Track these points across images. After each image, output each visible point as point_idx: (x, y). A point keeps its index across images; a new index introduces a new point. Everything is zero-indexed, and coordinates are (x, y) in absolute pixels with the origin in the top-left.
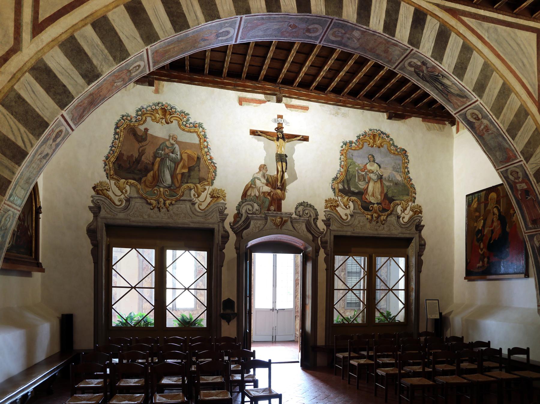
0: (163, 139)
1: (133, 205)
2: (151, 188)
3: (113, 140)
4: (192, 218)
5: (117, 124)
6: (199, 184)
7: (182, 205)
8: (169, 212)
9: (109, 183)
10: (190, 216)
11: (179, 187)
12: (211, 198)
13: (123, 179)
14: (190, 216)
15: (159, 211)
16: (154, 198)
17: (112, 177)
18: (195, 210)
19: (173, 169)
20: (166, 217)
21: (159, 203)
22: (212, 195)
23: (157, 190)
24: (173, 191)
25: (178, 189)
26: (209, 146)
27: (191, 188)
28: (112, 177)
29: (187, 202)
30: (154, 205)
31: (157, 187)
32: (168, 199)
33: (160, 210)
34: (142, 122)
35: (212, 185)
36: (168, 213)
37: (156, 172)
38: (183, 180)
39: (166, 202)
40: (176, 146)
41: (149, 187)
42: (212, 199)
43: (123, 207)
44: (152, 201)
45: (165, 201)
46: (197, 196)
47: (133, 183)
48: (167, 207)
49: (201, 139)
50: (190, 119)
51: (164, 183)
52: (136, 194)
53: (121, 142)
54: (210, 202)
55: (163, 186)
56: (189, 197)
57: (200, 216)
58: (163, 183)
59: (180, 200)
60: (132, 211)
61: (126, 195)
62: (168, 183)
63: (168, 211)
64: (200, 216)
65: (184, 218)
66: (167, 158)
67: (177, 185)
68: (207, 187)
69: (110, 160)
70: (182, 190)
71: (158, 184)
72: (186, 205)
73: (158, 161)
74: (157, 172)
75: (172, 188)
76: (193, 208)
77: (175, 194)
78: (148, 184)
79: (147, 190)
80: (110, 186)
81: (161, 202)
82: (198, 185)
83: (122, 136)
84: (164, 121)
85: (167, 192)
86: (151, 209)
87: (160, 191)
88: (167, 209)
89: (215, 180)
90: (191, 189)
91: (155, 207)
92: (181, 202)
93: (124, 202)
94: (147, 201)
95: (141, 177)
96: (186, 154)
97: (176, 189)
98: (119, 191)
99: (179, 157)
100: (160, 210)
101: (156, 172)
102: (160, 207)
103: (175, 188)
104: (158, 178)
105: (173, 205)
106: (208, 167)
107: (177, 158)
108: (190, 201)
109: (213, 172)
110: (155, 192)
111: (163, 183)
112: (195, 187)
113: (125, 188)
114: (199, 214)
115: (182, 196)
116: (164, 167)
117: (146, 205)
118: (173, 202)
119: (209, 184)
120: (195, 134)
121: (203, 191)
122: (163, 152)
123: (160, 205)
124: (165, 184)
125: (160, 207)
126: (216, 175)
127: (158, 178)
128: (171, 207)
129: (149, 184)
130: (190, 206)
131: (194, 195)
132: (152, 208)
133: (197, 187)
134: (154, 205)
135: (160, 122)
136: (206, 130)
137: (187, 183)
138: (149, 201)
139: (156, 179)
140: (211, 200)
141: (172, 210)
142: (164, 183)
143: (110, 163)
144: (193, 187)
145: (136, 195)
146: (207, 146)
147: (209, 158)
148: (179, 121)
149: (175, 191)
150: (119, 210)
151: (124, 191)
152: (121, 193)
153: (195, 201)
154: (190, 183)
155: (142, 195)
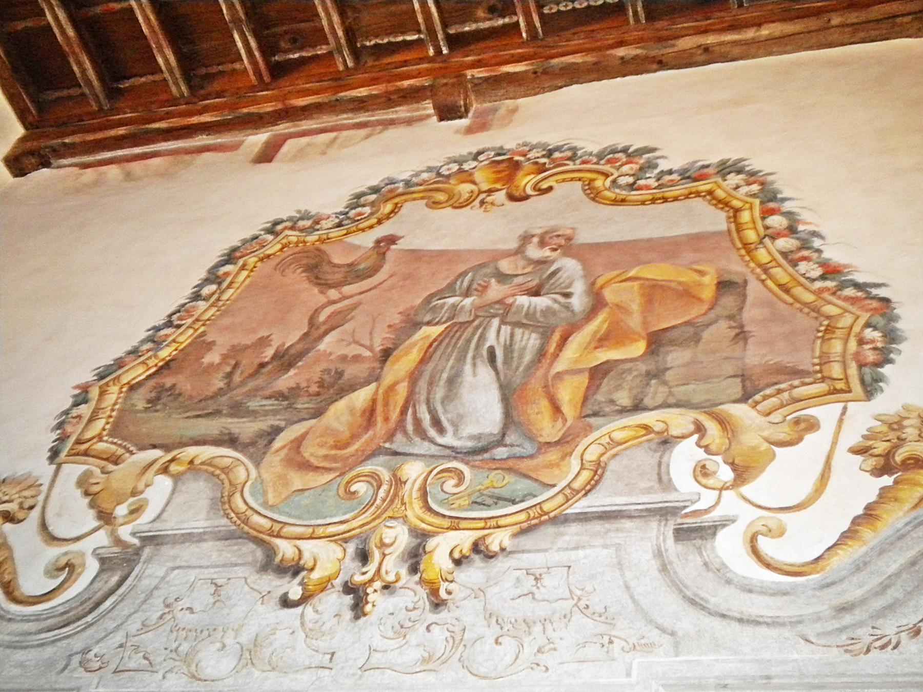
0: (483, 252)
1: (146, 583)
2: (329, 470)
3: (184, 305)
4: (676, 645)
5: (234, 250)
6: (745, 398)
7: (573, 555)
8: (443, 615)
9: (46, 481)
10: (663, 630)
11: (566, 442)
12: (879, 472)
13: (154, 447)
14: (663, 630)
15: (348, 615)
16: (332, 530)
17: (83, 447)
18: (722, 574)
19: (527, 358)
20: (413, 655)
21: (364, 557)
22: (888, 456)
23: (375, 480)
24: (510, 470)
25: (553, 455)
26: (801, 228)
27: (674, 432)
28: (83, 447)
29: (627, 524)
30: (316, 575)
31: (382, 459)
32: (455, 524)
33: (358, 608)
34: (375, 221)
35: (870, 388)
36: (432, 617)
37: (392, 388)
38: (600, 397)
39: (431, 544)
40: (570, 266)
41: (316, 469)
42: (887, 480)
43: (61, 609)
44: (307, 546)
45: (420, 536)
46: (726, 474)
47: (209, 463)
48: (430, 575)
49: (737, 211)
50: (659, 161)
51: (441, 430)
52: (203, 515)
53: (221, 303)
54: (868, 508)
55: (434, 450)
56: (649, 490)
57: (774, 623)
58: (432, 433)
59: (560, 520)
60: (117, 628)
61: (124, 532)
62: (470, 429)
63: (438, 604)
64: (774, 623)
65: (592, 651)
66: (494, 316)
67: (549, 430)
68: (826, 413)
69: (118, 378)
70: (589, 456)
71: (399, 443)
72: (618, 548)
73: (428, 337)
74: (402, 390)
75: (501, 452)
76: (695, 560)
77: (521, 486)
78: (311, 451)
79: (298, 485)
80: (41, 498)
81: (382, 545)
82: (740, 412)
83: (236, 285)
84: (500, 196)
85: (452, 482)
86: (286, 603)
87: (398, 482)
88: (434, 592)
89: (890, 361)
90: (666, 442)
91: (324, 585)
92: (574, 528)
93: (93, 566)
94: (270, 552)
95: (282, 424)
96: (636, 284)
97: (531, 457)
98: (92, 513)
99: (579, 302)
100: (358, 608)
101: (392, 388)
102: (371, 581)
103: (529, 448)
104: (404, 412)
105: (490, 556)
106: (817, 310)
107: (567, 307)
108: (664, 513)
109: (868, 325)
110: (360, 487)
111: (432, 433)
112: (712, 428)
113: (134, 493)
114: (757, 606)
115: (589, 489)
116: (462, 359)
117: (253, 577)
118: (497, 540)
119: (836, 391)
120: (698, 204)
121: (782, 437)
122: (468, 301)
123: (371, 568)
124: (448, 439)
125: (371, 581)
126: (892, 337)
127: (404, 412)
128: (474, 574)
129: (323, 452)
130: (659, 554)
131: (702, 472)
132: (295, 592)
133: (723, 422)
134: (316, 575)
135: (477, 202)
136: (784, 200)
137: (637, 407)
138: (285, 549)
139: (386, 419)
140: (884, 491)
141: (479, 592)
142: (441, 430)
143: (114, 389)
144: (692, 427)
145: (199, 522)
146: (792, 230)
147: (817, 272)
148: (592, 180)
149: (523, 465)
150: (26, 627)
151: (121, 511)
152: (96, 524)
153: (716, 514)
154: (666, 405)
155: (246, 521)
